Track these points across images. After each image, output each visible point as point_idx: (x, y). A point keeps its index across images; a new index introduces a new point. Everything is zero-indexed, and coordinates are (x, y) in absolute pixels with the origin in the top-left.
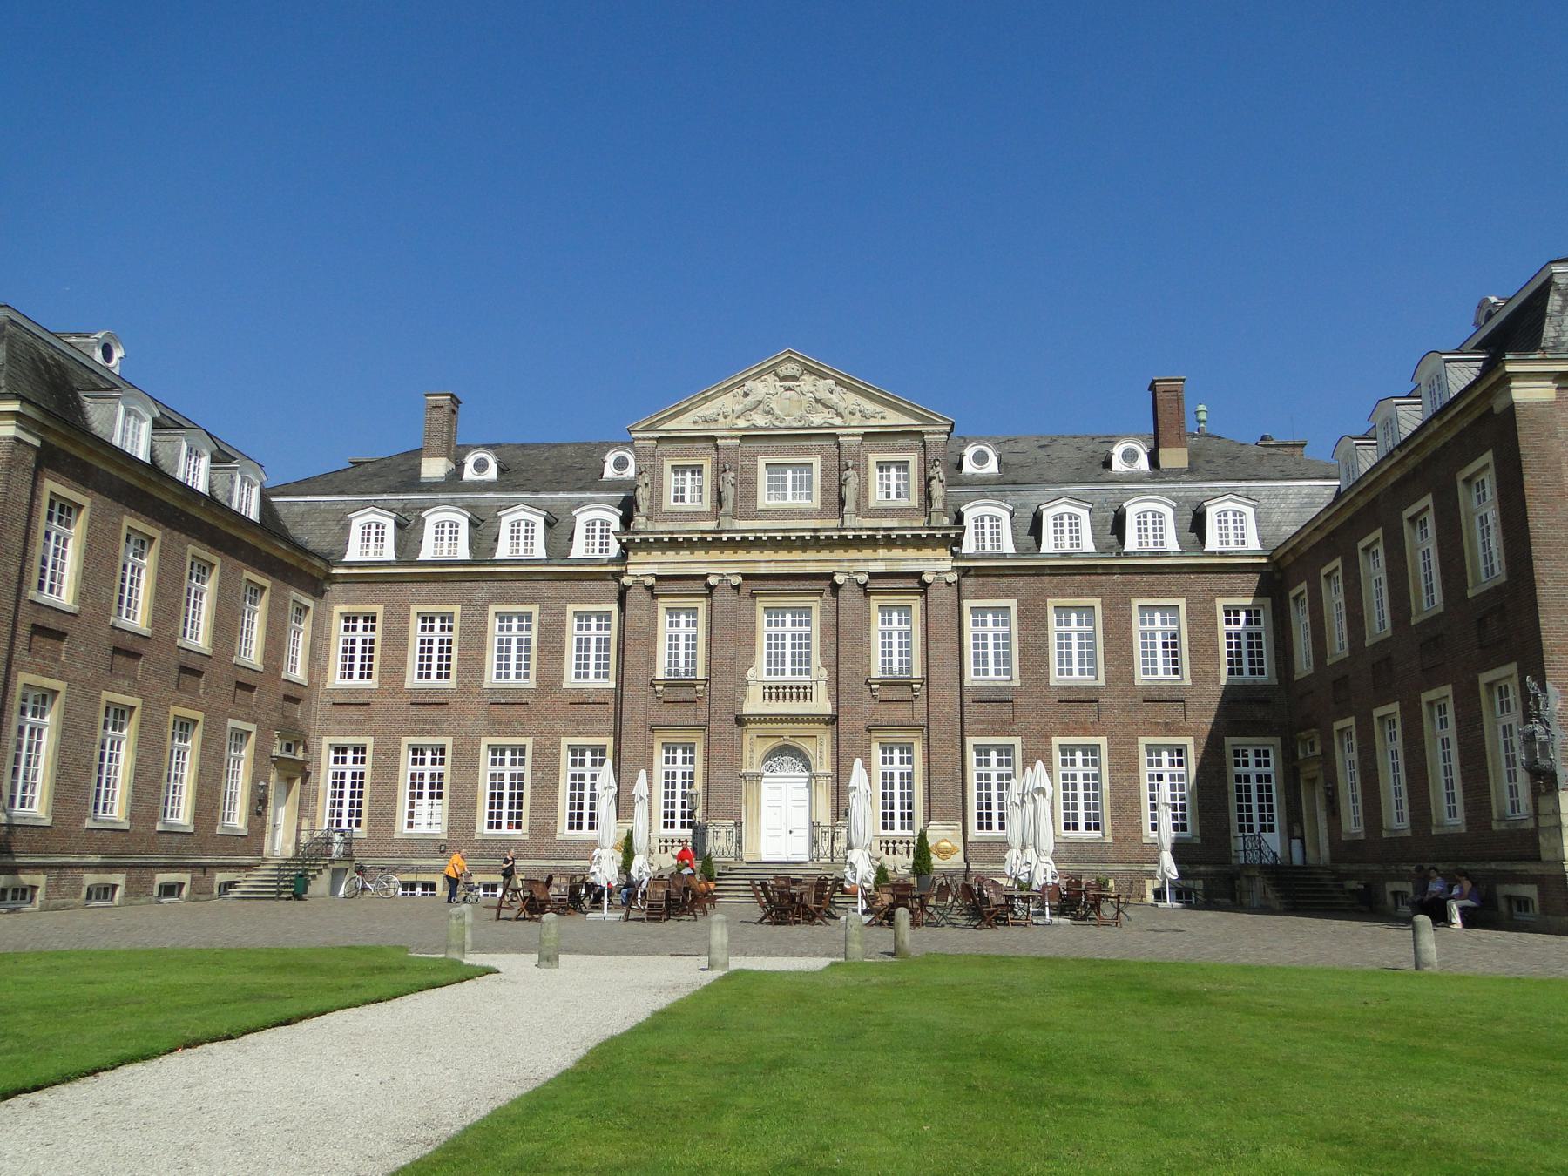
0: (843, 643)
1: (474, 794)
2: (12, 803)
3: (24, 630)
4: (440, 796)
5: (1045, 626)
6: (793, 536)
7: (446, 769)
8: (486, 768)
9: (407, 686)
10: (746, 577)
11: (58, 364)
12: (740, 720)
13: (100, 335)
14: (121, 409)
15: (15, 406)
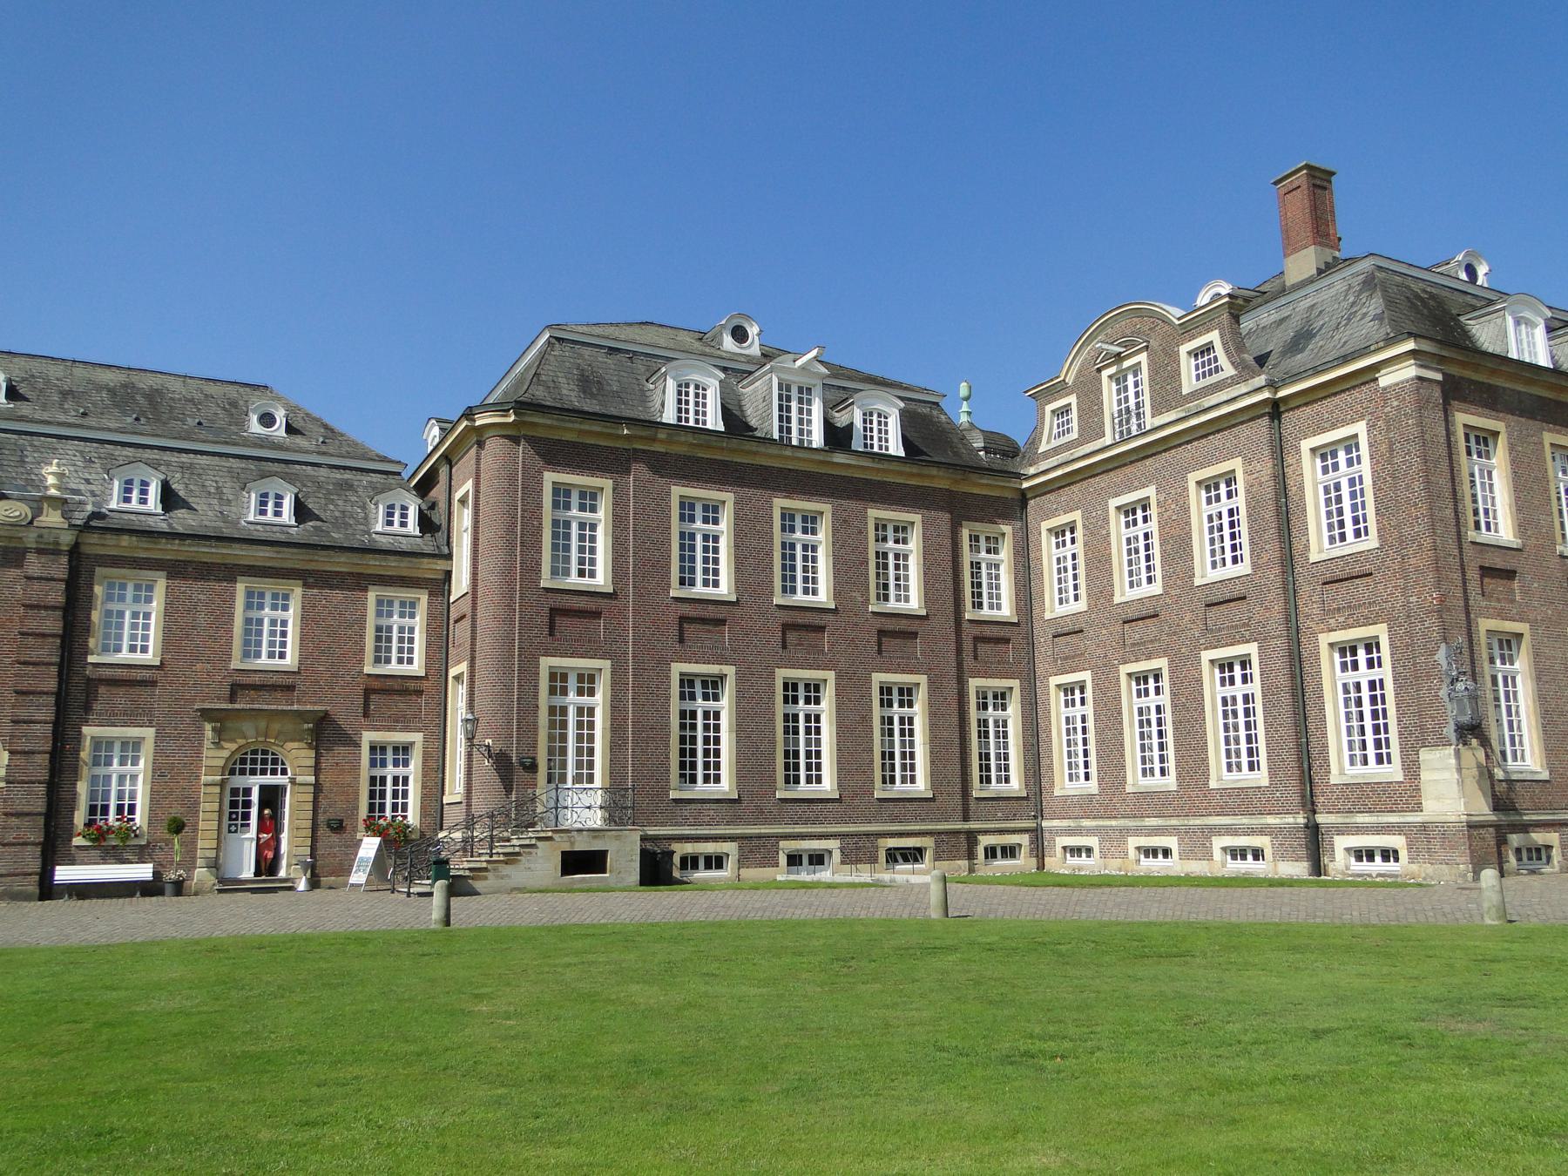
2: (1505, 760)
3: (1473, 574)
11: (1432, 296)
13: (1460, 257)
14: (1510, 321)
15: (1410, 345)
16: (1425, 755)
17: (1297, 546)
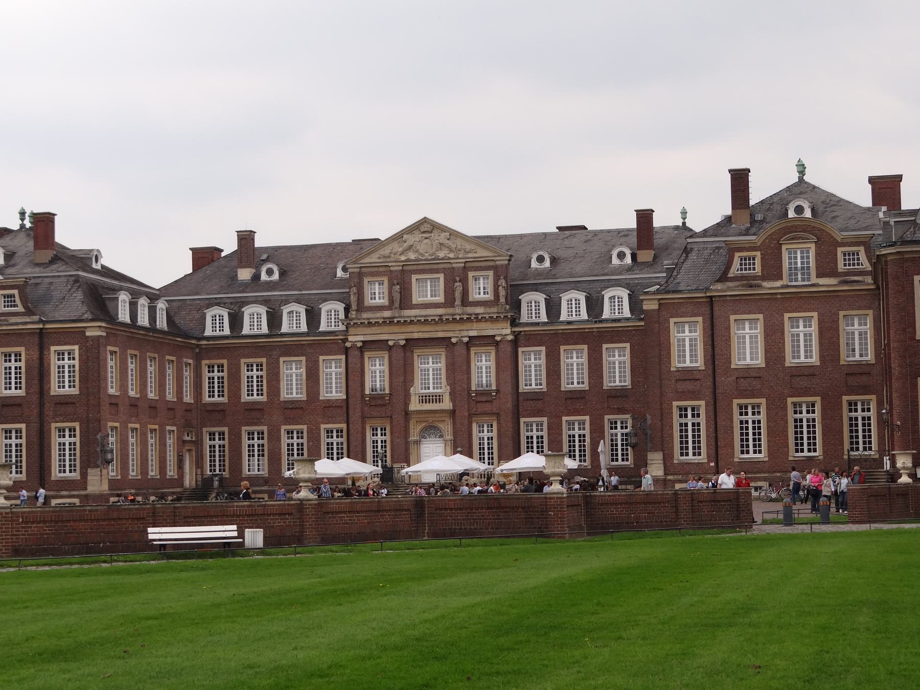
0: (458, 372)
1: (280, 454)
4: (263, 455)
5: (559, 360)
6: (430, 319)
7: (265, 442)
8: (285, 440)
9: (242, 401)
10: (406, 340)
12: (407, 414)
16: (89, 470)
17: (46, 387)
